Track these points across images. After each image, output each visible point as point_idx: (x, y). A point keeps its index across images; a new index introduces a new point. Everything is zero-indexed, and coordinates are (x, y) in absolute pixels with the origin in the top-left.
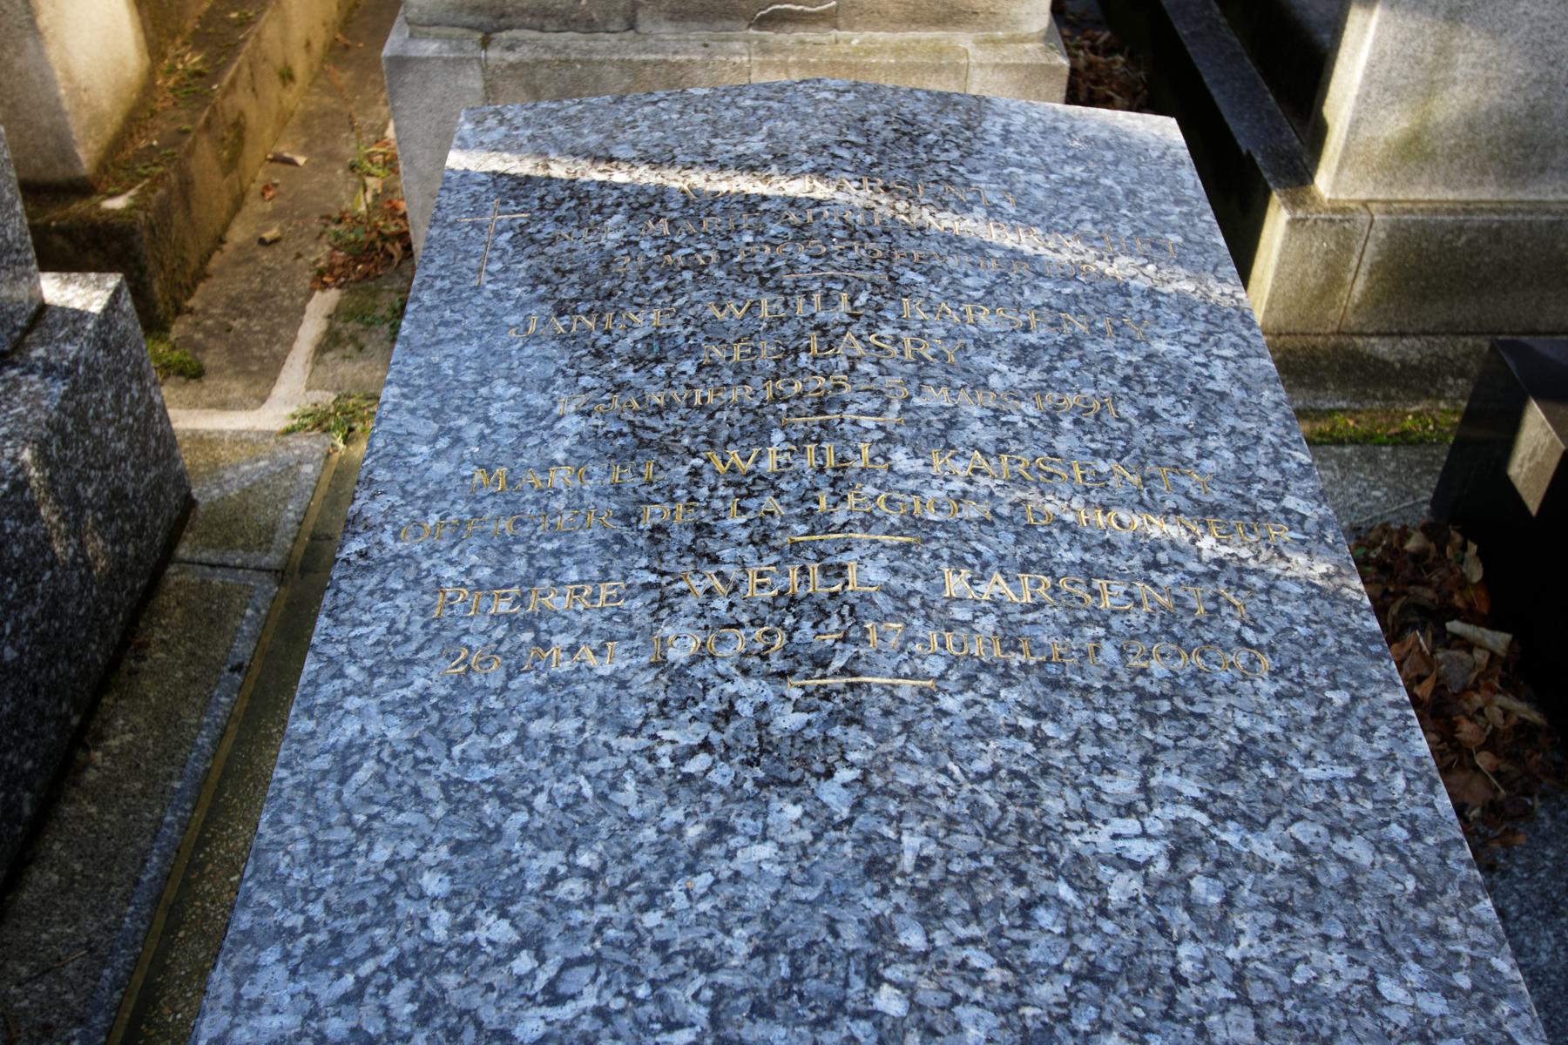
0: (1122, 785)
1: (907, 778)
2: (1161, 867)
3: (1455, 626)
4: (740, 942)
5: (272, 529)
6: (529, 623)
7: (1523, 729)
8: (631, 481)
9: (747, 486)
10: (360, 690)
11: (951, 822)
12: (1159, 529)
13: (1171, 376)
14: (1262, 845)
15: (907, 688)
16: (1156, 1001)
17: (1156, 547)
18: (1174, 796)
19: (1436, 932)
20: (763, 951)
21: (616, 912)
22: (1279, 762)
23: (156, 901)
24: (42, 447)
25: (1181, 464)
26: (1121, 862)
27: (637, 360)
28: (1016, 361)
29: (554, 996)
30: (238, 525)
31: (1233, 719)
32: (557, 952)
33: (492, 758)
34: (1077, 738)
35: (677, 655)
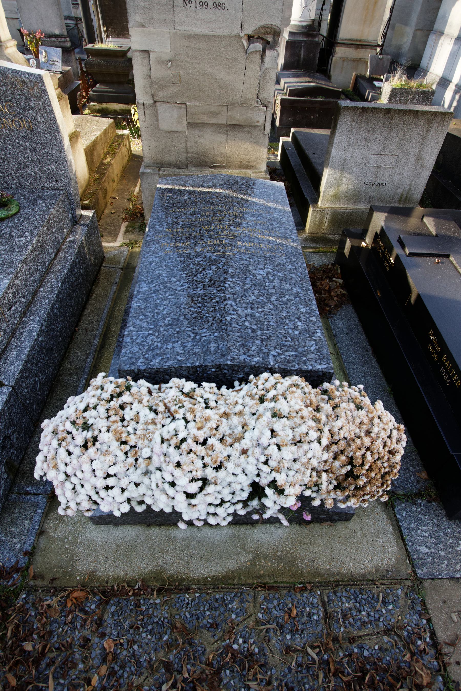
0: (261, 267)
1: (230, 264)
2: (265, 275)
3: (334, 279)
4: (207, 280)
5: (120, 262)
6: (176, 247)
7: (343, 295)
8: (190, 230)
9: (208, 231)
10: (151, 255)
11: (236, 269)
12: (271, 238)
13: (276, 219)
14: (280, 274)
15: (231, 254)
16: (262, 288)
17: (270, 241)
18: (268, 268)
19: (302, 284)
20: (210, 281)
21: (191, 278)
22: (284, 266)
23: (107, 315)
24: (85, 237)
25: (276, 231)
26: (259, 274)
27: (191, 215)
28: (251, 216)
29: (182, 286)
30: (114, 261)
31: (277, 261)
32: (182, 281)
33: (172, 262)
34: (255, 261)
35: (198, 251)
